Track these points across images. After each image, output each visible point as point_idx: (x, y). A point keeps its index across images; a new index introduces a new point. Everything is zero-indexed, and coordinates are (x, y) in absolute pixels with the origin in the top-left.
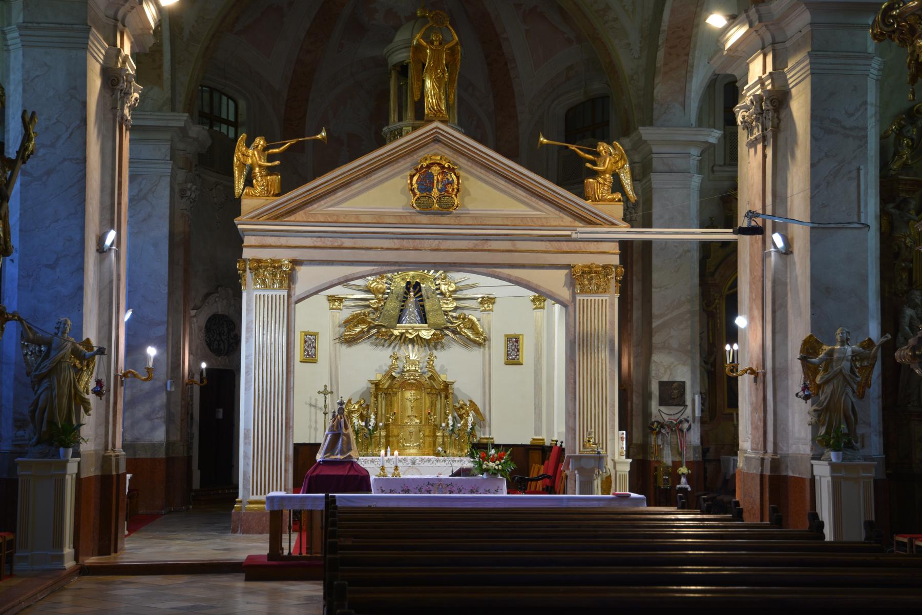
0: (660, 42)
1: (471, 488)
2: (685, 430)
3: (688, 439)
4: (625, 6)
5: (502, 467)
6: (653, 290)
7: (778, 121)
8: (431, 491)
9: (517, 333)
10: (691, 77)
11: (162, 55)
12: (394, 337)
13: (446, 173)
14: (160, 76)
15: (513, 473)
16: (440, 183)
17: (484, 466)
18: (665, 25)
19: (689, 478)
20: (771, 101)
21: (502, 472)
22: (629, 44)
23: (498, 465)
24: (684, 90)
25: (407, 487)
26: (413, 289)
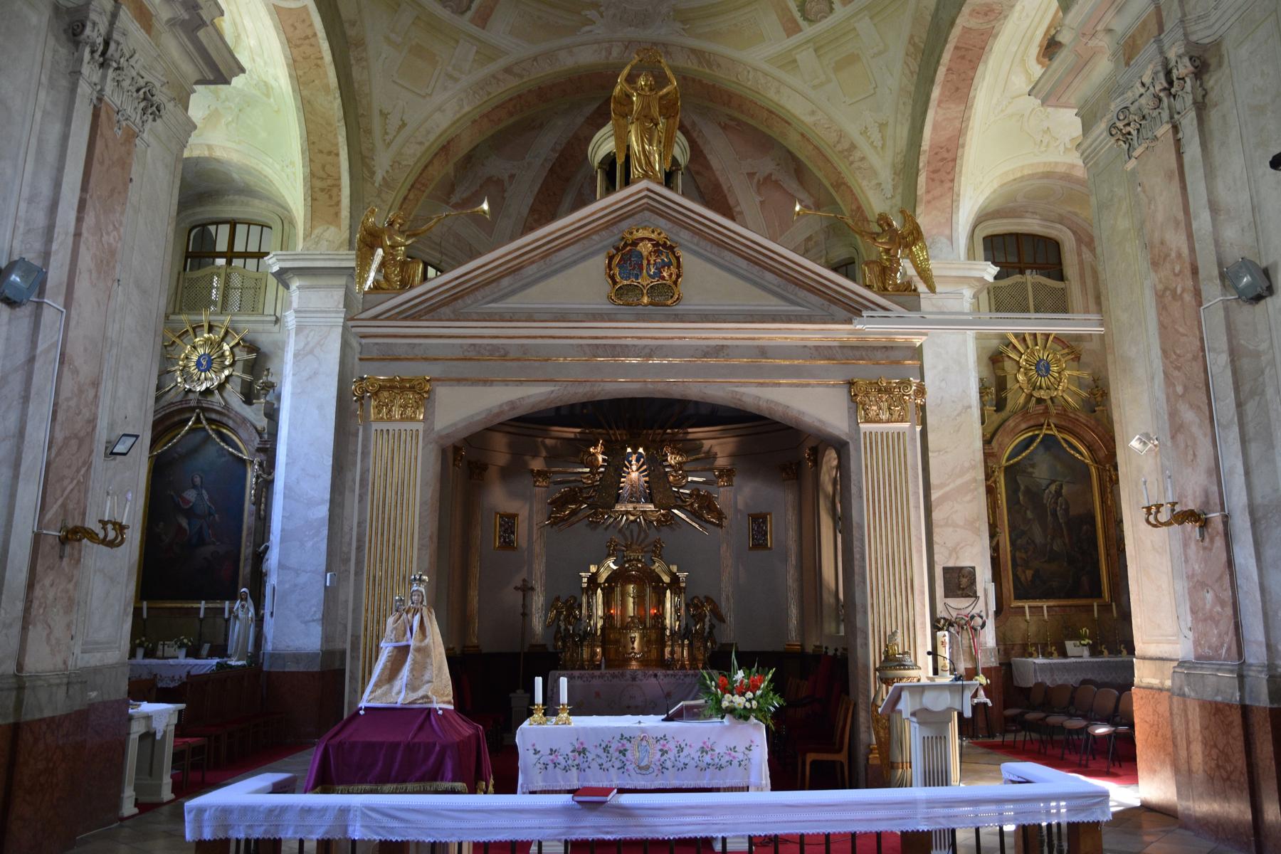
0: (921, 165)
1: (701, 745)
2: (979, 628)
3: (982, 639)
4: (872, 142)
5: (758, 702)
6: (930, 454)
7: (1204, 92)
8: (626, 750)
9: (764, 511)
10: (958, 207)
11: (340, 190)
13: (661, 253)
14: (337, 214)
15: (778, 716)
16: (651, 267)
17: (725, 704)
18: (926, 145)
19: (987, 690)
20: (1190, 59)
21: (760, 713)
23: (749, 700)
24: (950, 222)
25: (582, 744)
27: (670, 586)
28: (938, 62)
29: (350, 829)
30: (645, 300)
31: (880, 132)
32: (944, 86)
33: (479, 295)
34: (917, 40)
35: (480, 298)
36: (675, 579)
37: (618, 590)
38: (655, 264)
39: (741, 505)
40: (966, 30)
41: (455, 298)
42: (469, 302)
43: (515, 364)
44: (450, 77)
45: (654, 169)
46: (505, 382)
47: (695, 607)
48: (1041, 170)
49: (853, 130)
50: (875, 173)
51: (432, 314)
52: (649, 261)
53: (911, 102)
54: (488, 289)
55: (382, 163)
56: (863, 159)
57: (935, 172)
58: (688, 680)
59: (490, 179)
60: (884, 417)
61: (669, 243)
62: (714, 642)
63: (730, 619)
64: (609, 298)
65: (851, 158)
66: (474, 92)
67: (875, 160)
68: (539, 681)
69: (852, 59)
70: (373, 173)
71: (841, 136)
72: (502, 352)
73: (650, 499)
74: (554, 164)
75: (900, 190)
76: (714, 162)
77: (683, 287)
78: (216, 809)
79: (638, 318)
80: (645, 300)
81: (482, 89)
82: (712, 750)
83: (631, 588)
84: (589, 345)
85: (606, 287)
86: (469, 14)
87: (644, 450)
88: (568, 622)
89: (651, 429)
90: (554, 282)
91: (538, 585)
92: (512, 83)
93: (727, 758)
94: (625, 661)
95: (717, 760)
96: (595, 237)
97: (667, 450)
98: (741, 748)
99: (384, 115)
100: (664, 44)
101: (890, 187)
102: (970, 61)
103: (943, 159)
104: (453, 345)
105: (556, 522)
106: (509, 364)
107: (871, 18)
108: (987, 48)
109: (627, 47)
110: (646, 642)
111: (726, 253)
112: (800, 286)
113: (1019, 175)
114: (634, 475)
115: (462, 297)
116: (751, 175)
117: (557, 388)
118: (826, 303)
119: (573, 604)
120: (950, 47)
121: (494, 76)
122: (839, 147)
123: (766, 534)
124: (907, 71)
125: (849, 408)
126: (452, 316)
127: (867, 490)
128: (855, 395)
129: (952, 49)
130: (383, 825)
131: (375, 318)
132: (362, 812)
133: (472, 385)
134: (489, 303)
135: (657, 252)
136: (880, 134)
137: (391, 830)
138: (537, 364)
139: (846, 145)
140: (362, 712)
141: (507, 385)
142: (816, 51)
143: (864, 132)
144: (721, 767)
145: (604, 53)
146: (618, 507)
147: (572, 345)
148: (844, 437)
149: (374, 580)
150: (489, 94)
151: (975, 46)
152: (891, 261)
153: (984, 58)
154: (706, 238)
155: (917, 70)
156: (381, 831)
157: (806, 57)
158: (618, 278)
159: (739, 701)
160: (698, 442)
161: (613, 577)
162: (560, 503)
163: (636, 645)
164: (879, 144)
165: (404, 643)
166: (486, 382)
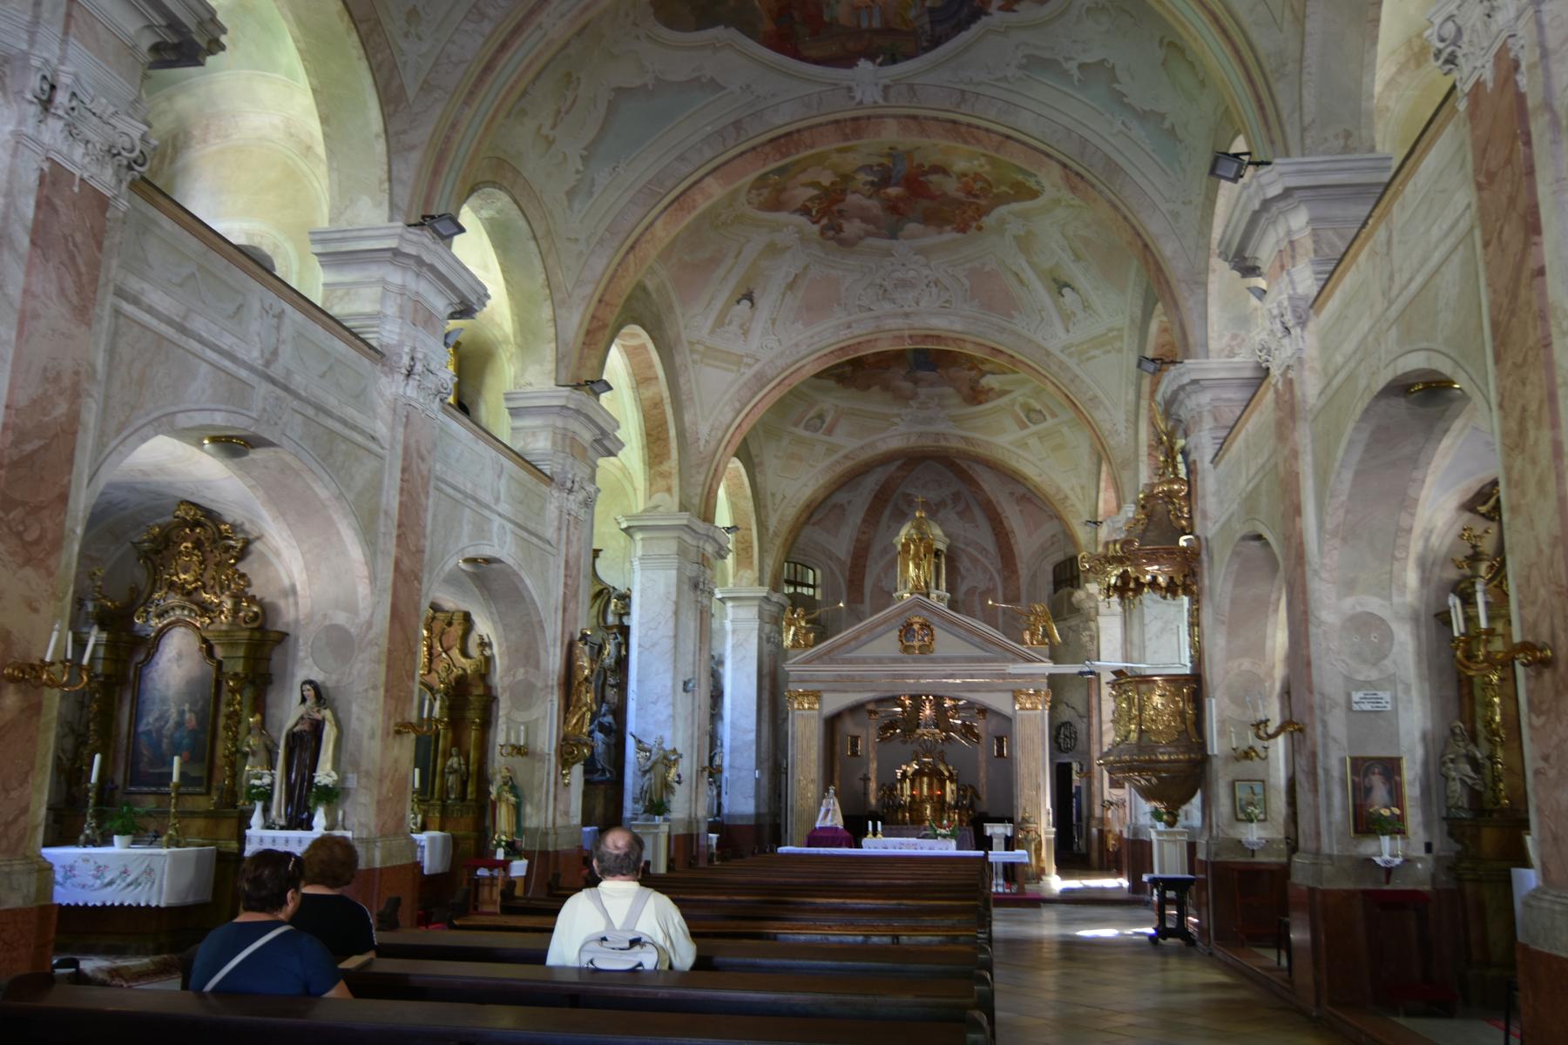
14: (751, 563)
27: (949, 778)
36: (951, 774)
37: (918, 780)
41: (829, 652)
46: (854, 691)
47: (962, 790)
49: (1065, 487)
55: (773, 522)
59: (835, 506)
62: (974, 811)
63: (984, 797)
68: (870, 823)
70: (767, 529)
73: (937, 726)
76: (985, 486)
79: (915, 661)
83: (925, 779)
88: (889, 797)
90: (876, 643)
91: (873, 776)
92: (849, 464)
99: (773, 495)
105: (882, 740)
110: (934, 810)
114: (928, 712)
116: (1012, 494)
119: (892, 788)
135: (922, 629)
146: (919, 731)
157: (1034, 442)
159: (943, 831)
161: (916, 773)
162: (884, 728)
163: (928, 812)
166: (846, 692)
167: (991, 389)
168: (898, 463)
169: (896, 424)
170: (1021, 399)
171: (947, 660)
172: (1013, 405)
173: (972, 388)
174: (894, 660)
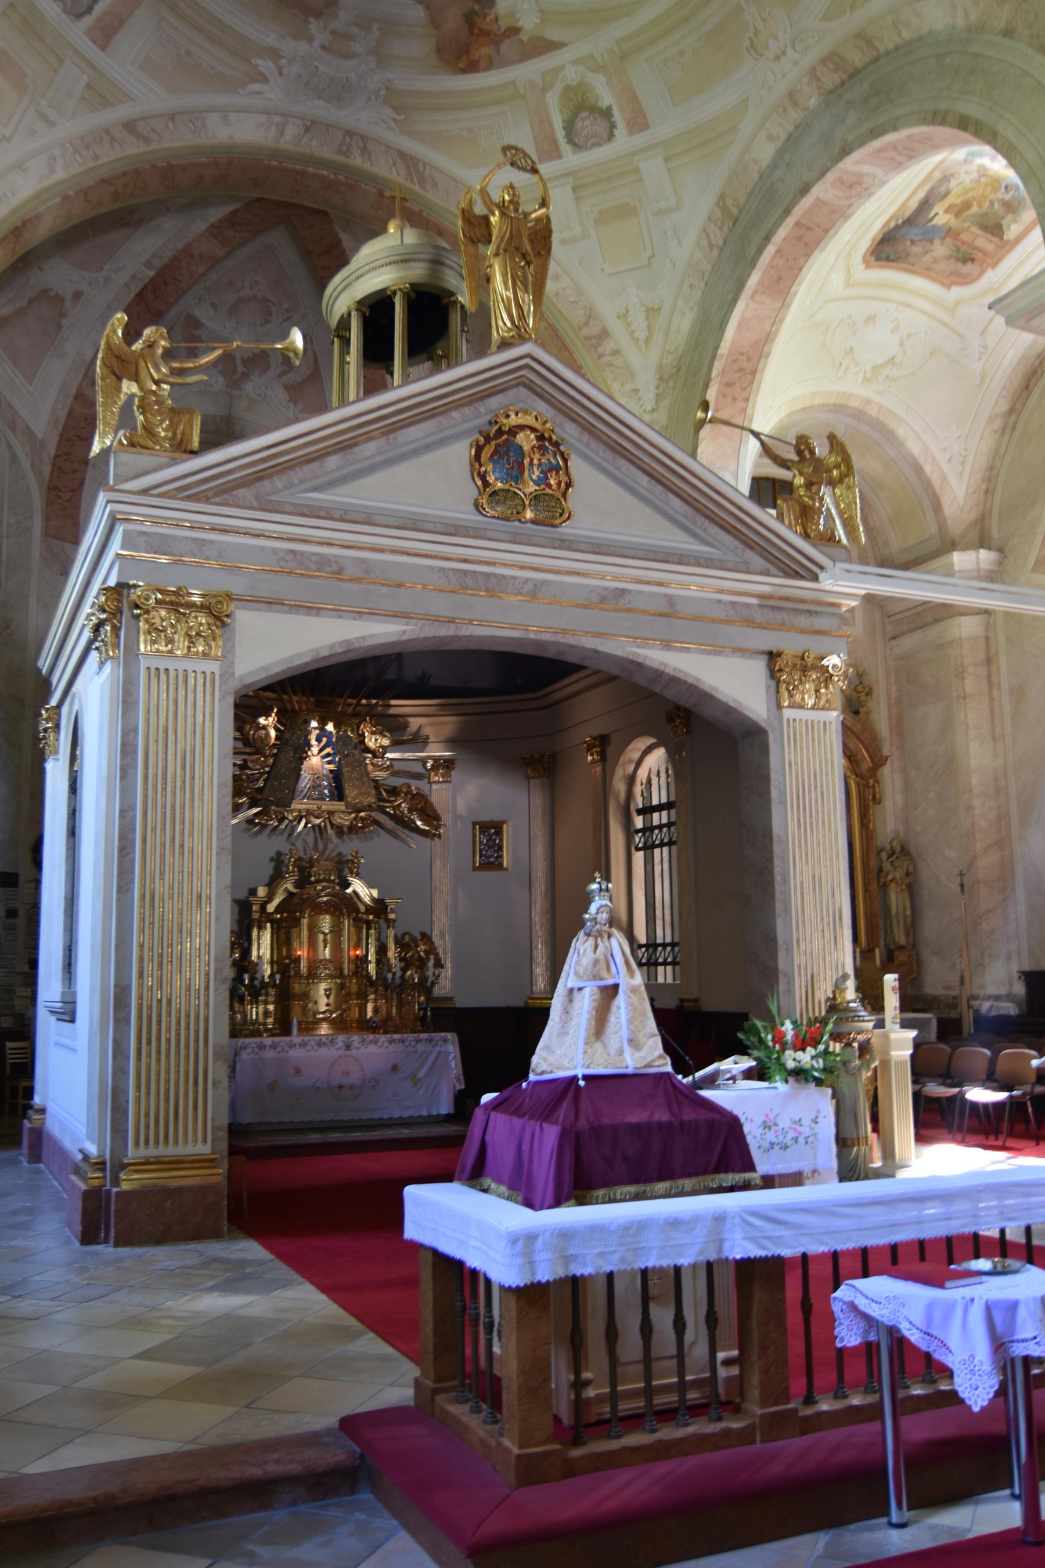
0: (714, 373)
1: (763, 1118)
4: (632, 332)
9: (497, 818)
12: (286, 822)
16: (535, 469)
17: (791, 1064)
22: (636, 391)
26: (316, 740)
28: (767, 239)
29: (727, 1245)
30: (529, 514)
31: (647, 318)
32: (765, 273)
33: (295, 475)
34: (729, 202)
35: (296, 481)
37: (305, 922)
38: (540, 465)
39: (462, 805)
40: (819, 203)
41: (259, 477)
42: (280, 486)
43: (354, 586)
44: (43, 117)
45: (528, 325)
46: (338, 612)
48: (832, 401)
49: (608, 311)
50: (632, 375)
51: (226, 496)
52: (532, 460)
53: (703, 285)
54: (307, 469)
56: (616, 352)
57: (729, 385)
58: (420, 1047)
59: (45, 292)
60: (810, 702)
61: (554, 438)
64: (477, 505)
65: (600, 350)
66: (76, 151)
67: (632, 355)
69: (625, 212)
71: (590, 316)
72: (335, 567)
74: (146, 286)
75: (667, 402)
77: (574, 501)
78: (552, 1235)
80: (529, 514)
81: (87, 147)
82: (776, 1125)
84: (454, 570)
85: (470, 490)
86: (88, 20)
87: (335, 727)
89: (341, 697)
90: (402, 472)
92: (134, 149)
93: (792, 1134)
94: (309, 1026)
95: (781, 1138)
96: (456, 414)
97: (366, 730)
98: (807, 1121)
100: (362, 137)
101: (651, 396)
102: (807, 245)
103: (741, 370)
104: (263, 549)
106: (346, 585)
107: (666, 160)
108: (832, 232)
109: (307, 129)
111: (623, 463)
112: (712, 520)
113: (808, 403)
115: (270, 476)
117: (409, 628)
118: (741, 546)
120: (790, 221)
121: (107, 131)
122: (586, 332)
123: (500, 848)
124: (705, 243)
125: (768, 687)
126: (255, 504)
127: (792, 795)
128: (780, 670)
129: (792, 225)
130: (768, 1234)
131: (145, 492)
132: (744, 1221)
133: (289, 612)
134: (314, 489)
135: (542, 449)
136: (646, 323)
137: (777, 1240)
138: (385, 590)
139: (596, 331)
140: (582, 1083)
141: (340, 617)
142: (575, 190)
143: (624, 316)
144: (785, 1147)
145: (273, 132)
147: (431, 567)
148: (763, 724)
149: (152, 900)
150: (96, 157)
151: (819, 226)
152: (814, 500)
153: (823, 243)
154: (597, 438)
155: (721, 243)
156: (766, 1243)
158: (491, 479)
160: (401, 719)
164: (643, 335)
165: (610, 981)
166: (312, 610)
167: (515, 31)
168: (216, 214)
169: (264, 79)
170: (571, 75)
171: (598, 548)
172: (544, 90)
173: (470, 19)
174: (456, 530)
